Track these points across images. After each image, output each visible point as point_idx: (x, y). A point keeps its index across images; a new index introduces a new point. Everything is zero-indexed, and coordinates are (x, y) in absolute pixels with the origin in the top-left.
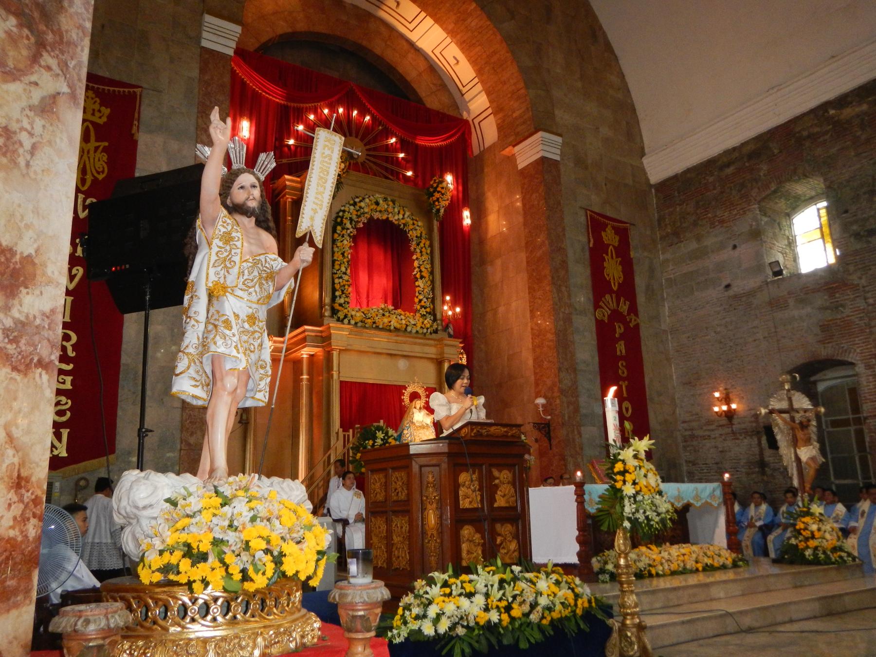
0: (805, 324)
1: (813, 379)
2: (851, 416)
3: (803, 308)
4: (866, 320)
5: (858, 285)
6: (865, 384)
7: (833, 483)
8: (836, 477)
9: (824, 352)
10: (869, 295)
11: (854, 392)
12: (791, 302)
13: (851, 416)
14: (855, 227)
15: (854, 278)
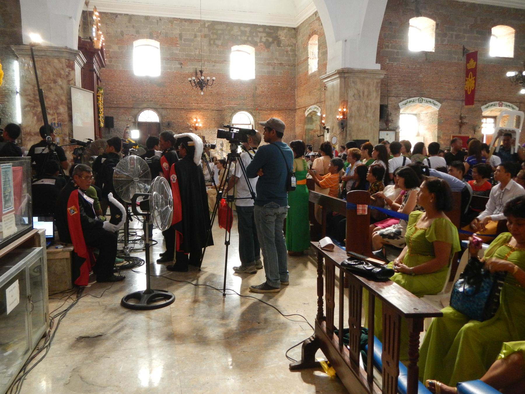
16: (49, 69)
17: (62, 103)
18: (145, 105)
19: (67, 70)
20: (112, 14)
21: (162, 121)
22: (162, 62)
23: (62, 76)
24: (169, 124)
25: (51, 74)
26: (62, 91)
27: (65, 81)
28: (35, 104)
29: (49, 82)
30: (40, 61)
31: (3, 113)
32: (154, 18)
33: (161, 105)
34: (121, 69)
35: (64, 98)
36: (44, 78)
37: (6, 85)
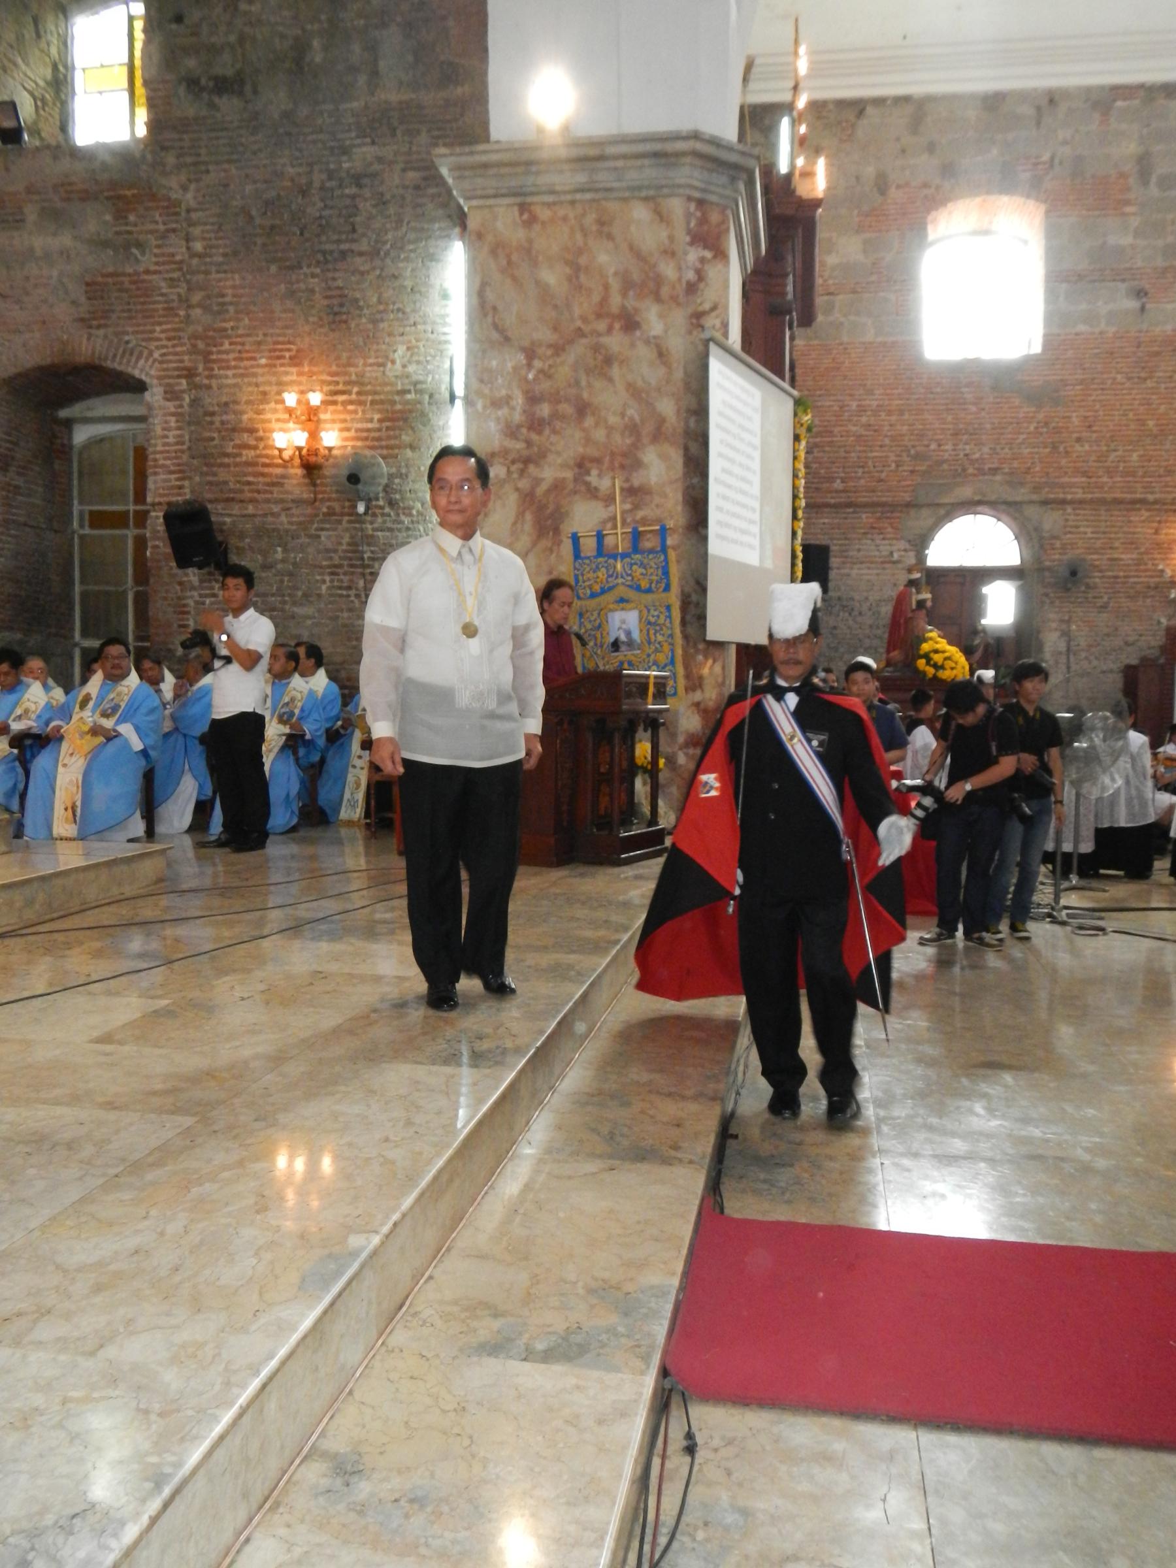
0: (55, 273)
1: (64, 413)
2: (132, 508)
3: (55, 234)
4: (182, 290)
5: (177, 204)
6: (159, 431)
7: (76, 645)
8: (85, 634)
9: (88, 346)
10: (196, 231)
11: (141, 454)
12: (31, 213)
13: (132, 508)
14: (191, 63)
15: (172, 185)
16: (603, 258)
17: (657, 436)
18: (966, 492)
19: (693, 255)
20: (841, 104)
21: (1038, 560)
22: (1051, 294)
23: (665, 291)
24: (1074, 573)
25: (615, 285)
26: (662, 371)
27: (679, 317)
28: (529, 443)
29: (602, 326)
30: (565, 219)
31: (392, 503)
32: (1023, 96)
33: (1037, 489)
34: (870, 336)
35: (667, 408)
36: (577, 312)
37: (411, 369)
